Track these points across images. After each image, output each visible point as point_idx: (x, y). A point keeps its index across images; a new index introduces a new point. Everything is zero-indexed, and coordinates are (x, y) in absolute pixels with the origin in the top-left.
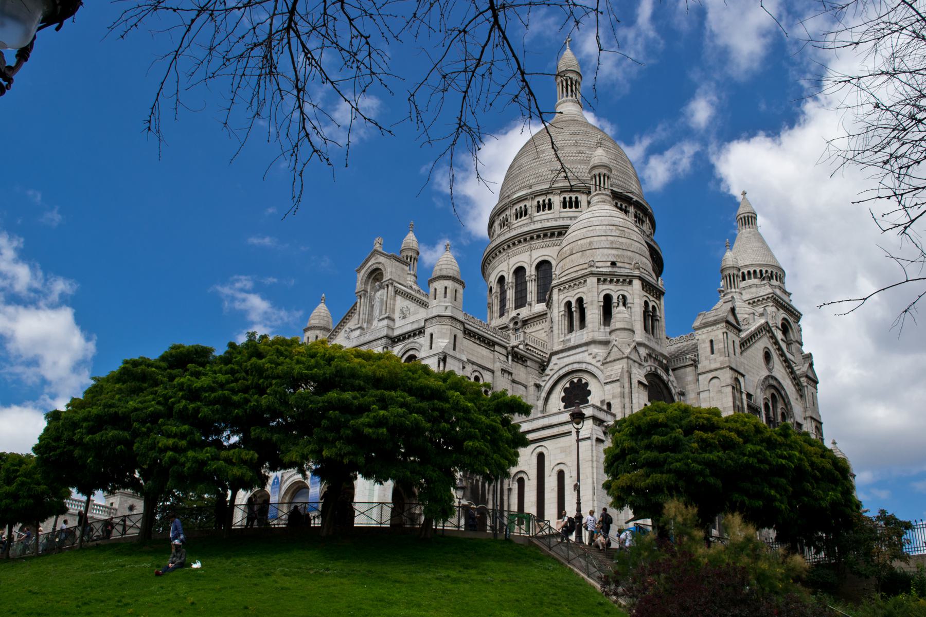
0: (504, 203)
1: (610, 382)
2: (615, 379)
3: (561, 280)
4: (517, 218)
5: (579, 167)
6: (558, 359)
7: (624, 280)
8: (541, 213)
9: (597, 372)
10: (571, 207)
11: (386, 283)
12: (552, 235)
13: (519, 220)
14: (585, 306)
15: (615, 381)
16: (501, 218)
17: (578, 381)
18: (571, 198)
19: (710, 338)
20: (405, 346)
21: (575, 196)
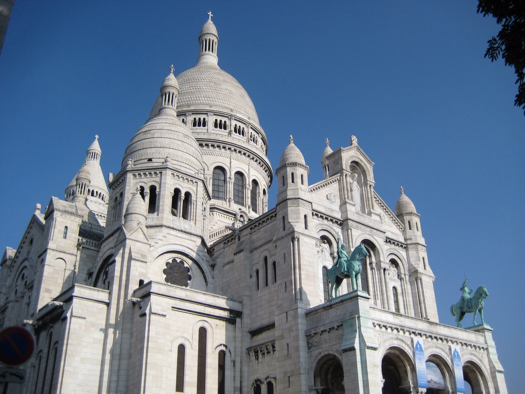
0: (225, 111)
11: (371, 184)
16: (219, 118)
20: (390, 249)
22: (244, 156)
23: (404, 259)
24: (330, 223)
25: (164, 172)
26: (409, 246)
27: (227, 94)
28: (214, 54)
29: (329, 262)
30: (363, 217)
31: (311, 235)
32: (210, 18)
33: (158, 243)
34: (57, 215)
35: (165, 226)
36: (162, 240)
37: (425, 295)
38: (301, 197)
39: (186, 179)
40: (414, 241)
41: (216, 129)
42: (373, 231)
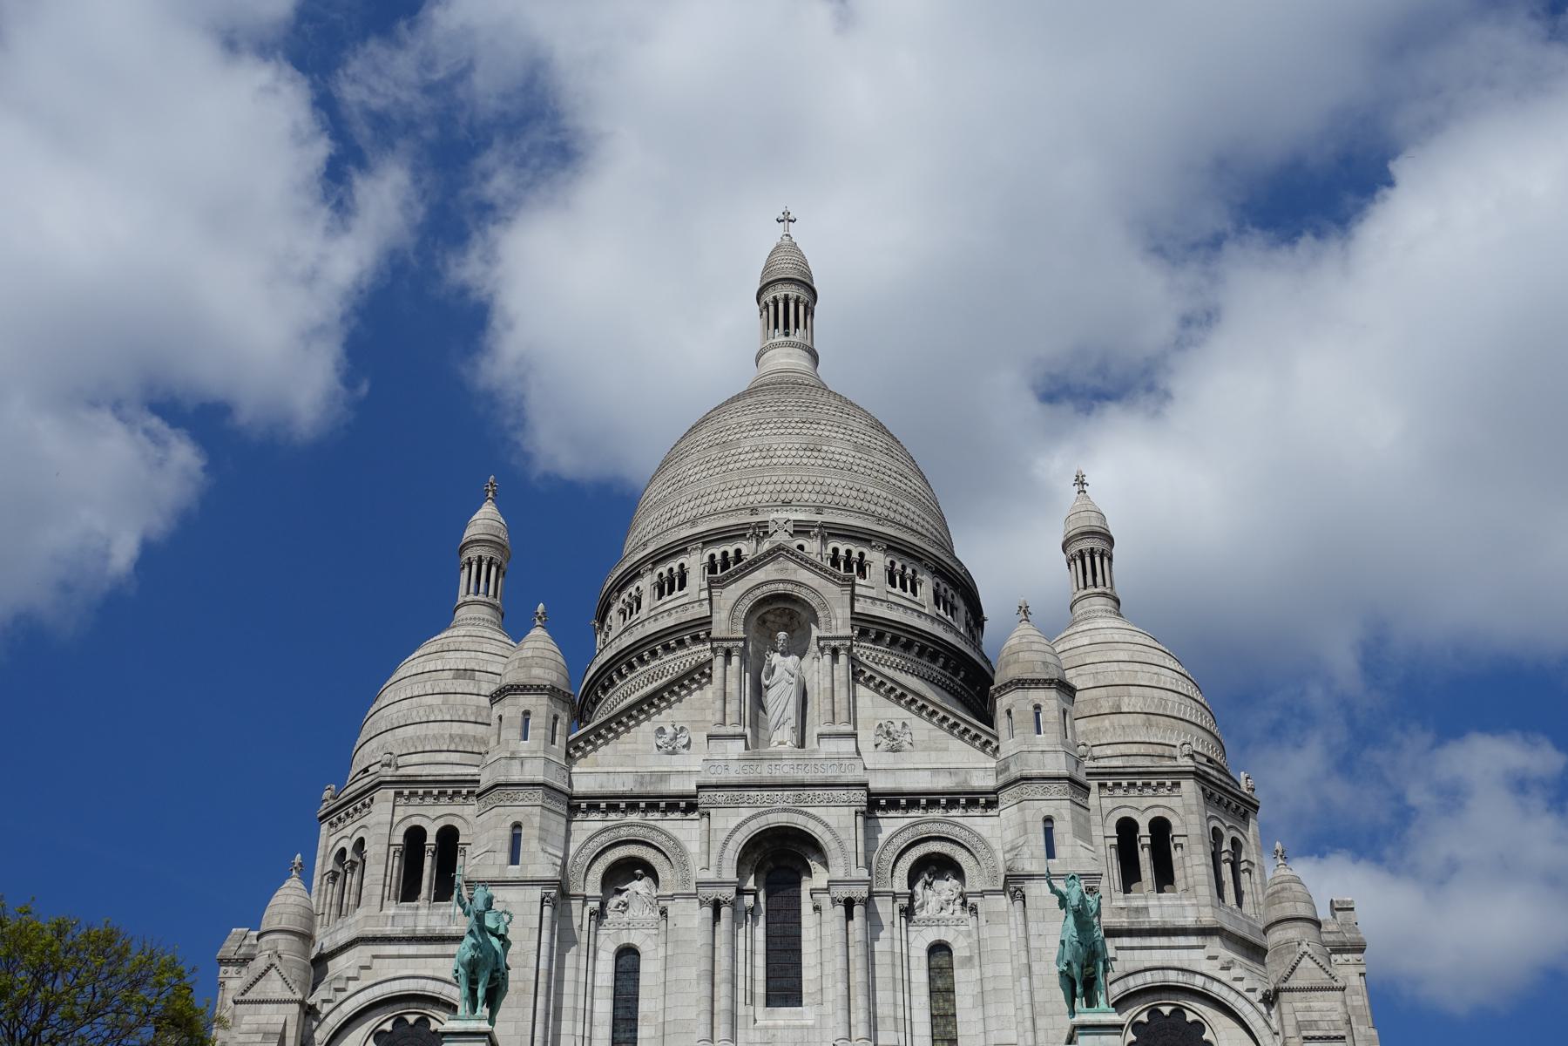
0: (732, 521)
1: (1321, 1038)
2: (1333, 1034)
3: (1102, 763)
5: (908, 506)
7: (1238, 808)
9: (1236, 1004)
11: (833, 643)
14: (1177, 840)
15: (1336, 1038)
16: (717, 552)
17: (1172, 1012)
18: (904, 567)
20: (914, 825)
23: (981, 840)
26: (1004, 797)
27: (752, 463)
29: (646, 931)
30: (766, 763)
31: (529, 876)
33: (344, 990)
34: (227, 975)
36: (356, 979)
37: (1033, 943)
38: (502, 779)
39: (439, 792)
40: (1015, 772)
42: (807, 793)
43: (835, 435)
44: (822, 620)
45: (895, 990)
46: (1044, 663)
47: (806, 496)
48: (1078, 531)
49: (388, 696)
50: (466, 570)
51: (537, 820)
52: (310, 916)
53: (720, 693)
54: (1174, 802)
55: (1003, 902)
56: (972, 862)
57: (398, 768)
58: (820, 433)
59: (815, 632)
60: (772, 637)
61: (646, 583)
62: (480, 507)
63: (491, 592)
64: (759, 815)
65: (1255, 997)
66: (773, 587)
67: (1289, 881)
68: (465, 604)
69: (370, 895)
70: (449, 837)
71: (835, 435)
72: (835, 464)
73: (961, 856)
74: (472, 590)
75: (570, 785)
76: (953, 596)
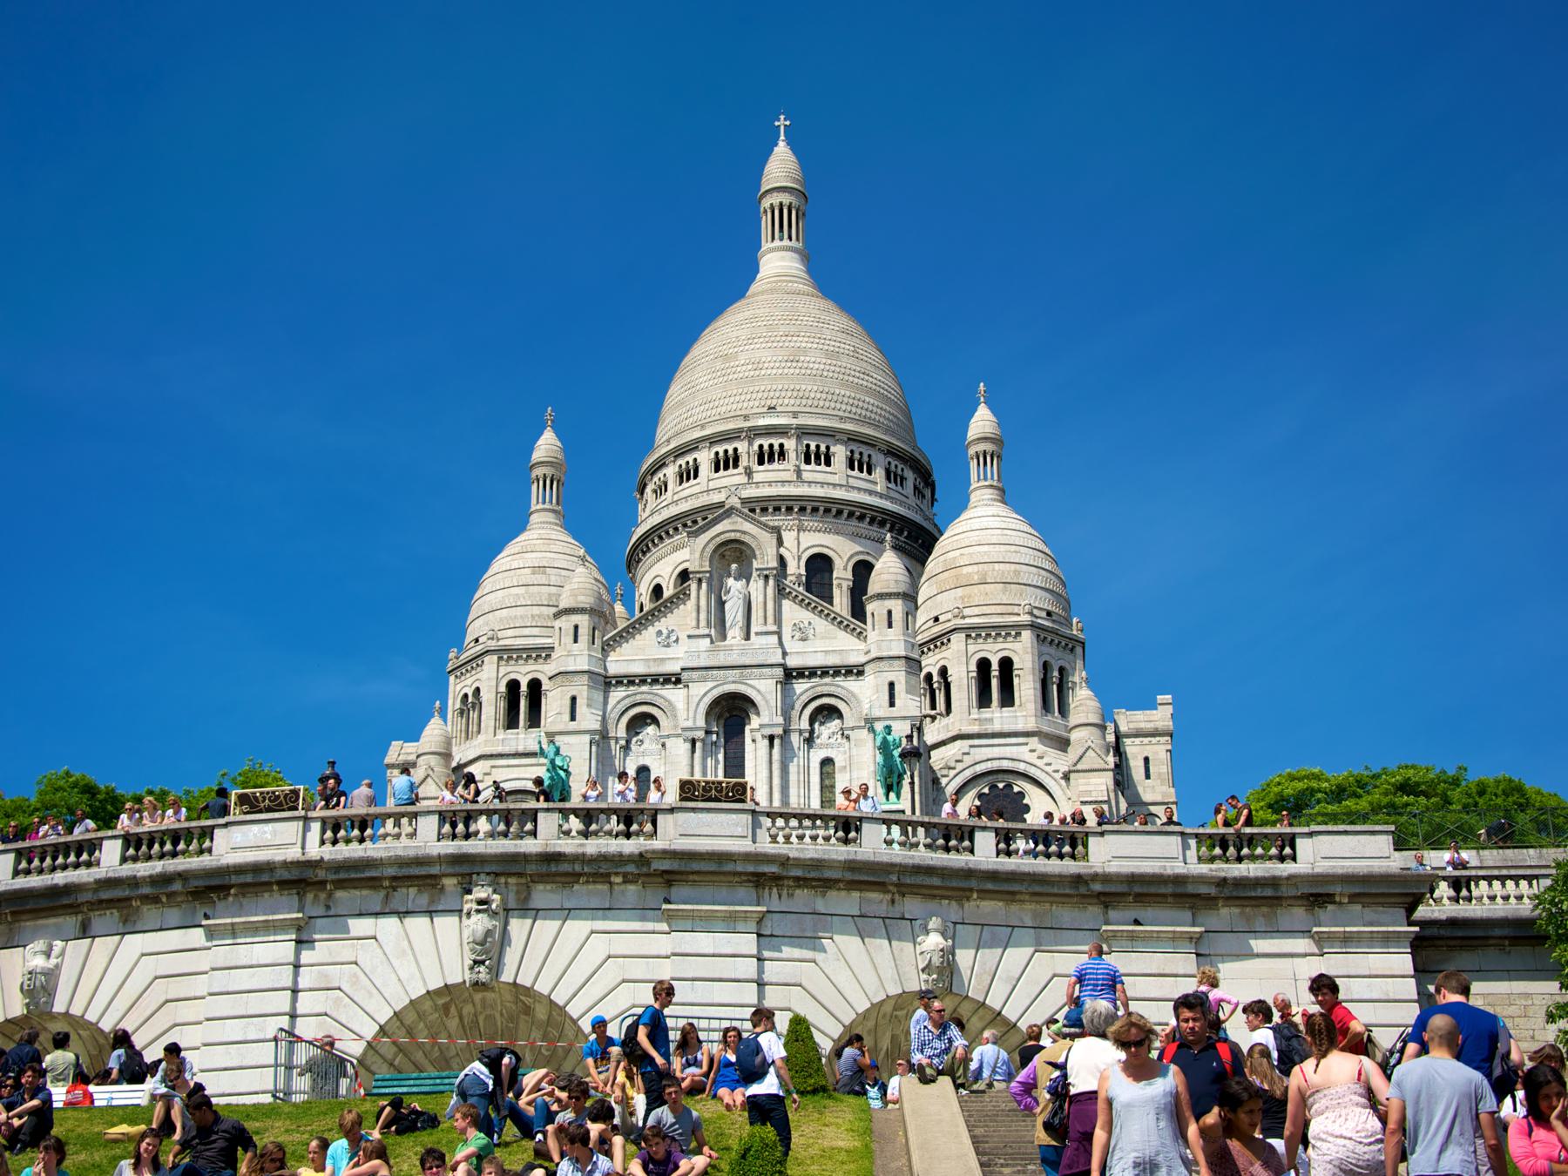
0: (731, 426)
3: (968, 621)
4: (761, 462)
5: (867, 399)
6: (971, 746)
7: (1067, 645)
8: (813, 466)
10: (862, 472)
11: (765, 572)
12: (840, 512)
13: (766, 466)
14: (1015, 672)
16: (720, 449)
17: (1005, 787)
18: (861, 454)
19: (1146, 754)
20: (813, 687)
21: (870, 452)
22: (777, 513)
23: (854, 695)
24: (657, 688)
25: (487, 659)
26: (867, 669)
27: (747, 374)
28: (786, 242)
30: (722, 653)
32: (782, 138)
35: (484, 756)
38: (562, 669)
40: (873, 655)
41: (717, 475)
43: (810, 345)
44: (758, 556)
45: (799, 787)
46: (896, 581)
47: (786, 401)
48: (975, 437)
49: (487, 584)
50: (536, 484)
51: (585, 694)
52: (448, 742)
53: (695, 607)
54: (1017, 646)
55: (865, 731)
56: (848, 709)
57: (498, 640)
58: (798, 345)
59: (755, 565)
60: (729, 565)
61: (670, 471)
62: (541, 434)
63: (554, 501)
64: (718, 686)
65: (1058, 776)
66: (727, 535)
67: (1086, 699)
68: (537, 511)
69: (487, 727)
70: (535, 686)
71: (810, 345)
72: (809, 372)
73: (841, 705)
74: (540, 500)
75: (605, 669)
76: (902, 470)
